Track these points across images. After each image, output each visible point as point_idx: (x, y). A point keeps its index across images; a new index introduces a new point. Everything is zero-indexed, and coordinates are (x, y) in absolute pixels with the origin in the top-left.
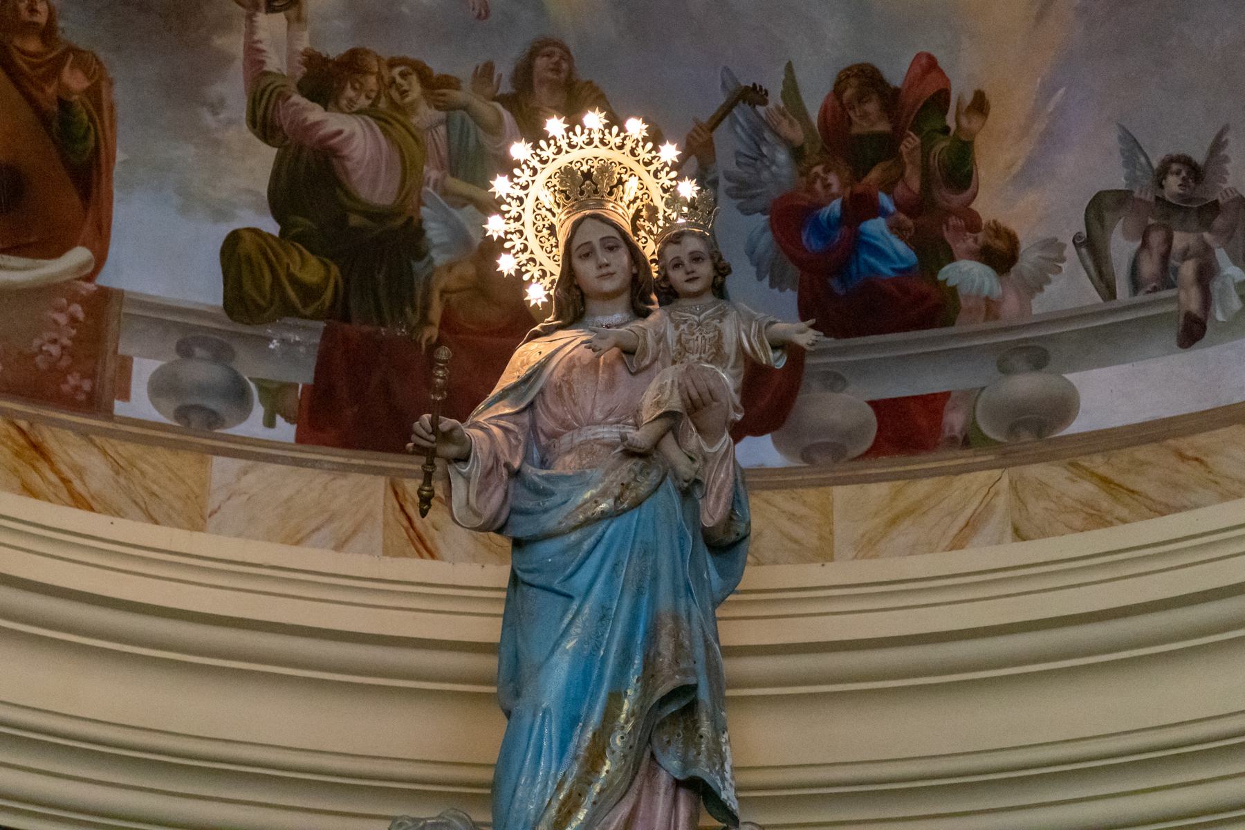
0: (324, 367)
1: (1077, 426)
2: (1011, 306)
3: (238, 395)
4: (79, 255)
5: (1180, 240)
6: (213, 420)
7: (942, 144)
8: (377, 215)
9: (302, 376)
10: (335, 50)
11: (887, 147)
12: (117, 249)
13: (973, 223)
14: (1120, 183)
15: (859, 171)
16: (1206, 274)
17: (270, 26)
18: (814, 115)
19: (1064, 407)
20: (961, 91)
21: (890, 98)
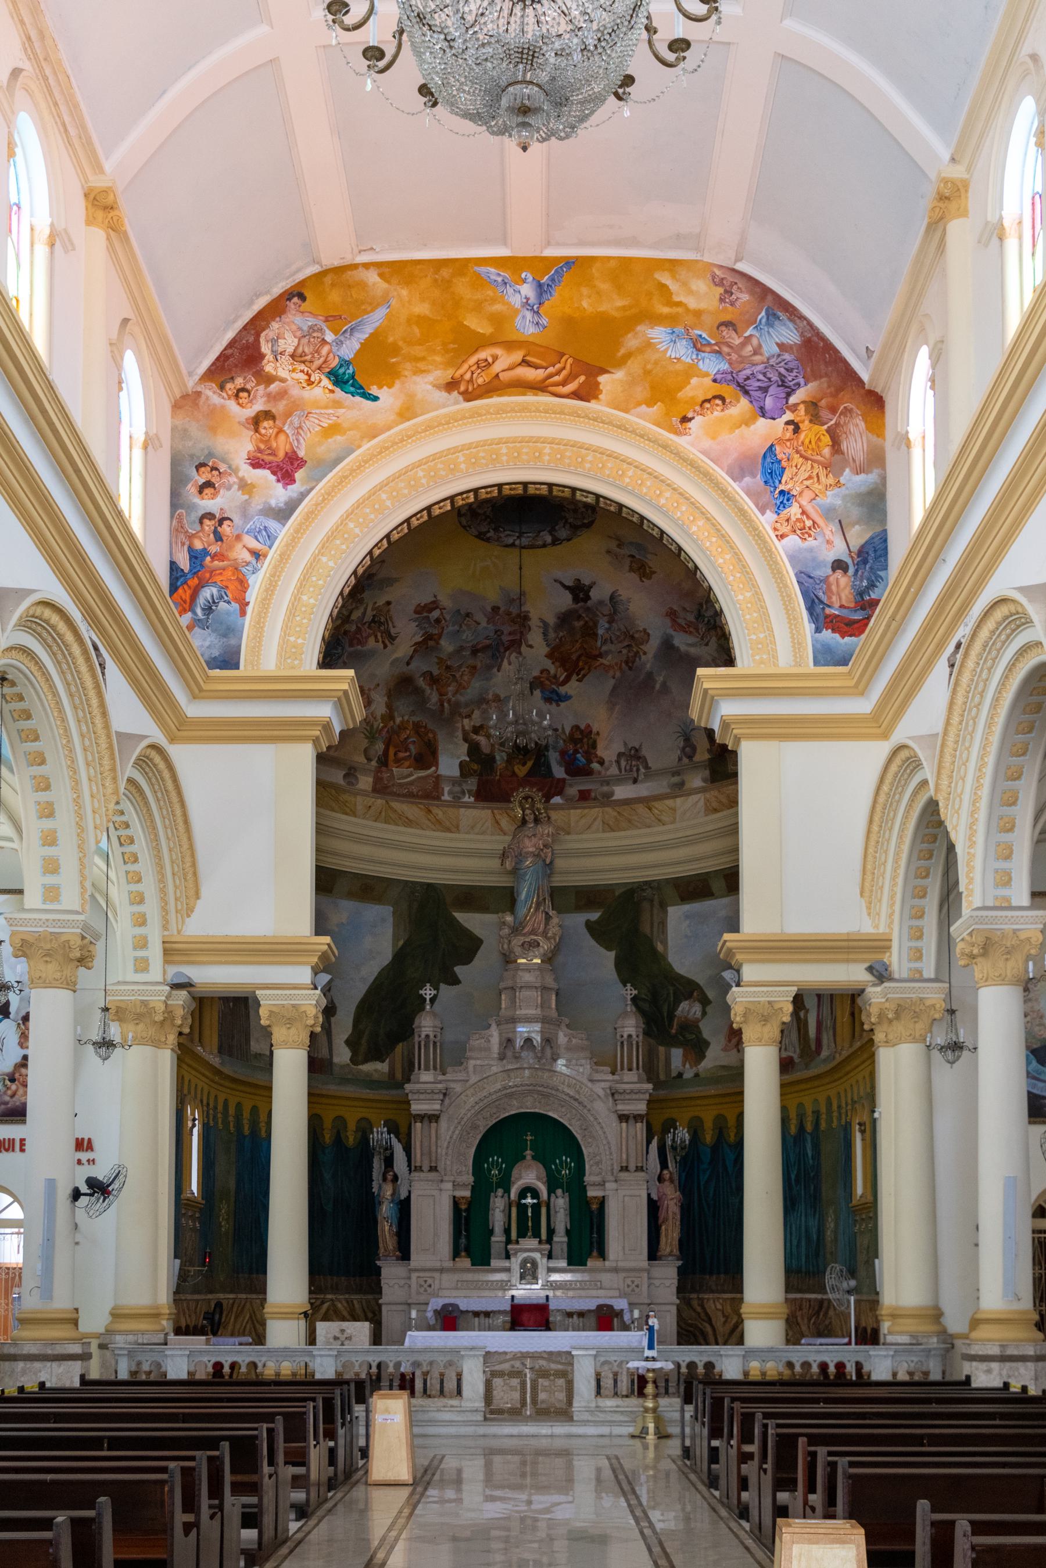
0: (478, 786)
1: (614, 798)
2: (603, 772)
3: (463, 793)
4: (433, 768)
5: (634, 763)
6: (460, 798)
7: (591, 741)
8: (486, 755)
9: (475, 788)
10: (478, 725)
11: (581, 740)
12: (440, 766)
13: (596, 756)
14: (623, 750)
15: (576, 745)
16: (638, 770)
17: (466, 721)
18: (567, 733)
19: (612, 794)
20: (595, 730)
21: (582, 732)
